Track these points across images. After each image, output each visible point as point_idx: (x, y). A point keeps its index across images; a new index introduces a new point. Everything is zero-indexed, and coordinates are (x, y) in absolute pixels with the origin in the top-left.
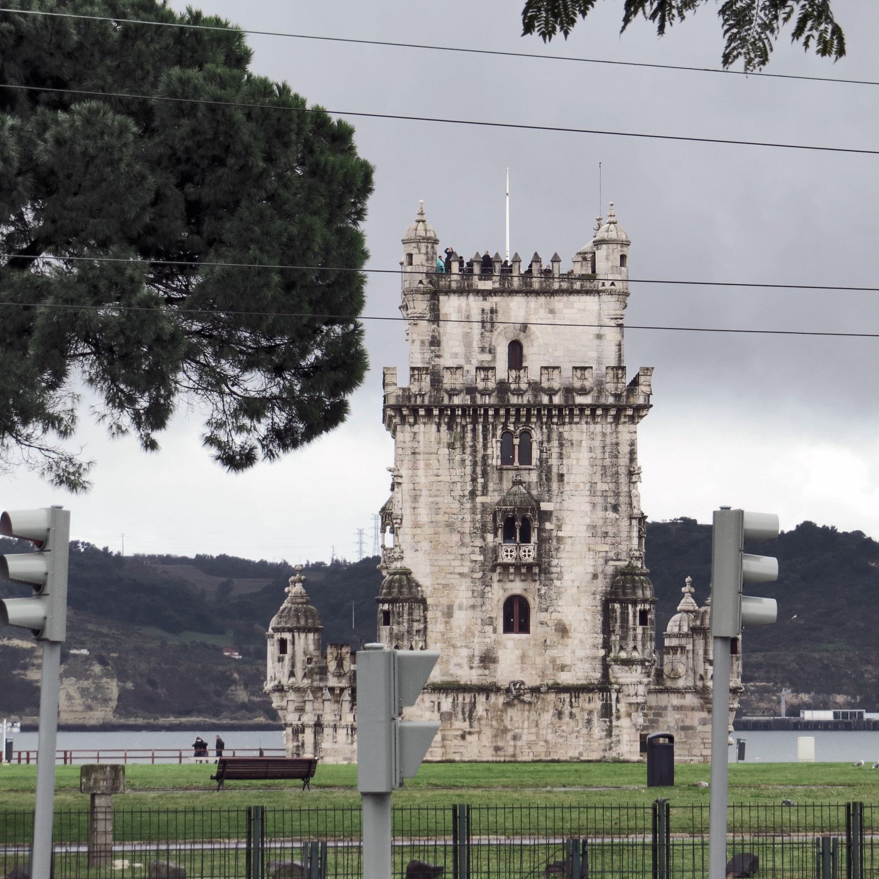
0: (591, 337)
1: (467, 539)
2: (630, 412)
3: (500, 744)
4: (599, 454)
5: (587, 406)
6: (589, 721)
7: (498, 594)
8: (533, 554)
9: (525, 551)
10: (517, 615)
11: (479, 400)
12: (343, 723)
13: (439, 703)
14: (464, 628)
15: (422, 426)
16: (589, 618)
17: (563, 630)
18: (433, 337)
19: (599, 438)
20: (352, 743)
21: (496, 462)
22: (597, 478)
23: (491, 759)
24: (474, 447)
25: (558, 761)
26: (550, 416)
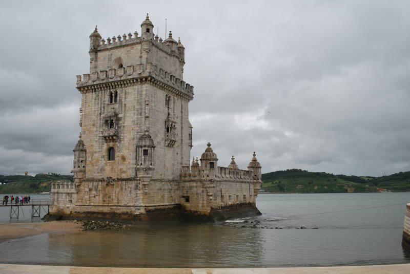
0: (138, 57)
1: (98, 129)
2: (144, 79)
3: (105, 199)
5: (131, 79)
6: (131, 191)
7: (105, 147)
8: (113, 132)
10: (111, 154)
17: (124, 158)
19: (136, 90)
20: (67, 198)
21: (107, 102)
22: (135, 104)
25: (120, 206)
26: (121, 85)
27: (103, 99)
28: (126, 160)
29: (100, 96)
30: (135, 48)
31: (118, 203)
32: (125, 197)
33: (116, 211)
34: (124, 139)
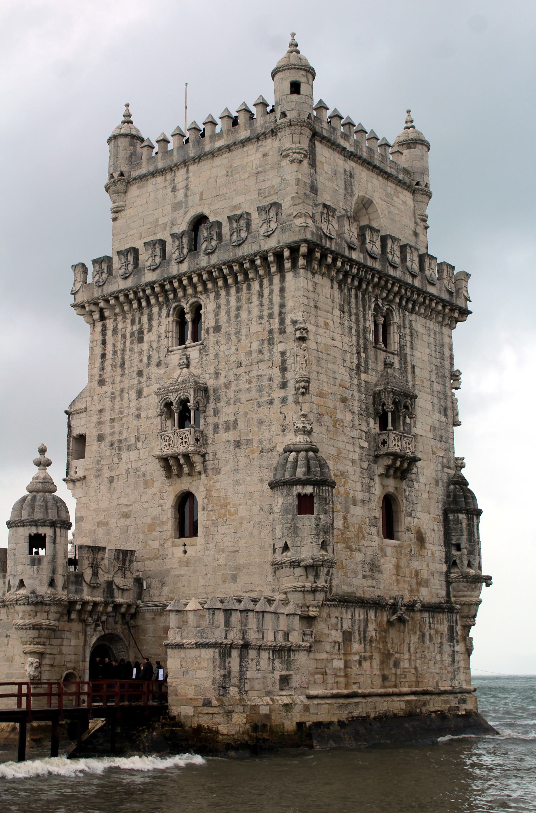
0: (411, 233)
1: (357, 422)
3: (386, 672)
4: (433, 354)
5: (437, 297)
9: (406, 443)
11: (370, 263)
12: (269, 644)
13: (342, 619)
14: (357, 526)
15: (320, 277)
16: (436, 528)
17: (421, 539)
18: (312, 181)
19: (432, 335)
20: (273, 670)
21: (371, 338)
23: (382, 691)
24: (357, 314)
27: (361, 320)
28: (427, 545)
29: (353, 305)
30: (401, 196)
31: (417, 683)
32: (432, 663)
33: (418, 710)
34: (417, 474)
